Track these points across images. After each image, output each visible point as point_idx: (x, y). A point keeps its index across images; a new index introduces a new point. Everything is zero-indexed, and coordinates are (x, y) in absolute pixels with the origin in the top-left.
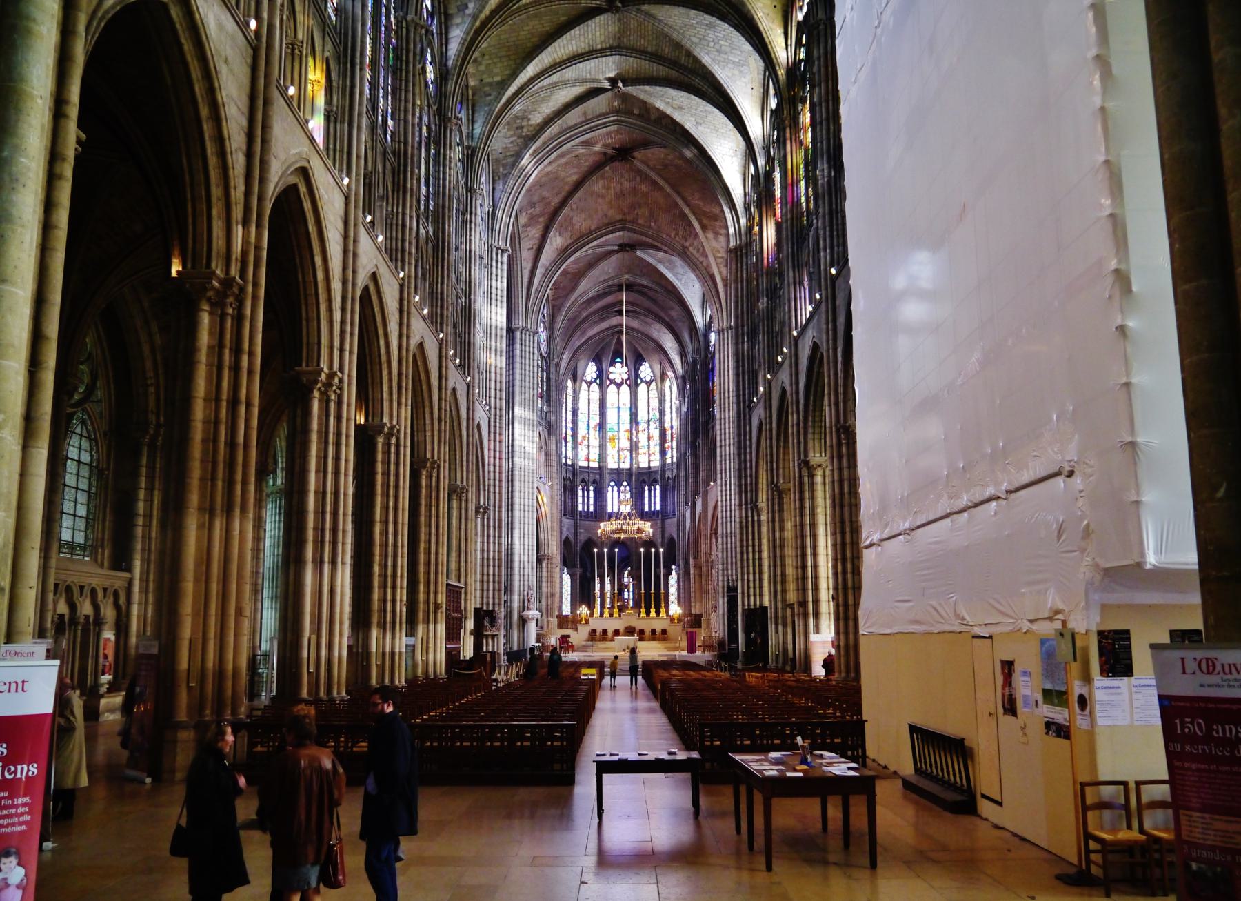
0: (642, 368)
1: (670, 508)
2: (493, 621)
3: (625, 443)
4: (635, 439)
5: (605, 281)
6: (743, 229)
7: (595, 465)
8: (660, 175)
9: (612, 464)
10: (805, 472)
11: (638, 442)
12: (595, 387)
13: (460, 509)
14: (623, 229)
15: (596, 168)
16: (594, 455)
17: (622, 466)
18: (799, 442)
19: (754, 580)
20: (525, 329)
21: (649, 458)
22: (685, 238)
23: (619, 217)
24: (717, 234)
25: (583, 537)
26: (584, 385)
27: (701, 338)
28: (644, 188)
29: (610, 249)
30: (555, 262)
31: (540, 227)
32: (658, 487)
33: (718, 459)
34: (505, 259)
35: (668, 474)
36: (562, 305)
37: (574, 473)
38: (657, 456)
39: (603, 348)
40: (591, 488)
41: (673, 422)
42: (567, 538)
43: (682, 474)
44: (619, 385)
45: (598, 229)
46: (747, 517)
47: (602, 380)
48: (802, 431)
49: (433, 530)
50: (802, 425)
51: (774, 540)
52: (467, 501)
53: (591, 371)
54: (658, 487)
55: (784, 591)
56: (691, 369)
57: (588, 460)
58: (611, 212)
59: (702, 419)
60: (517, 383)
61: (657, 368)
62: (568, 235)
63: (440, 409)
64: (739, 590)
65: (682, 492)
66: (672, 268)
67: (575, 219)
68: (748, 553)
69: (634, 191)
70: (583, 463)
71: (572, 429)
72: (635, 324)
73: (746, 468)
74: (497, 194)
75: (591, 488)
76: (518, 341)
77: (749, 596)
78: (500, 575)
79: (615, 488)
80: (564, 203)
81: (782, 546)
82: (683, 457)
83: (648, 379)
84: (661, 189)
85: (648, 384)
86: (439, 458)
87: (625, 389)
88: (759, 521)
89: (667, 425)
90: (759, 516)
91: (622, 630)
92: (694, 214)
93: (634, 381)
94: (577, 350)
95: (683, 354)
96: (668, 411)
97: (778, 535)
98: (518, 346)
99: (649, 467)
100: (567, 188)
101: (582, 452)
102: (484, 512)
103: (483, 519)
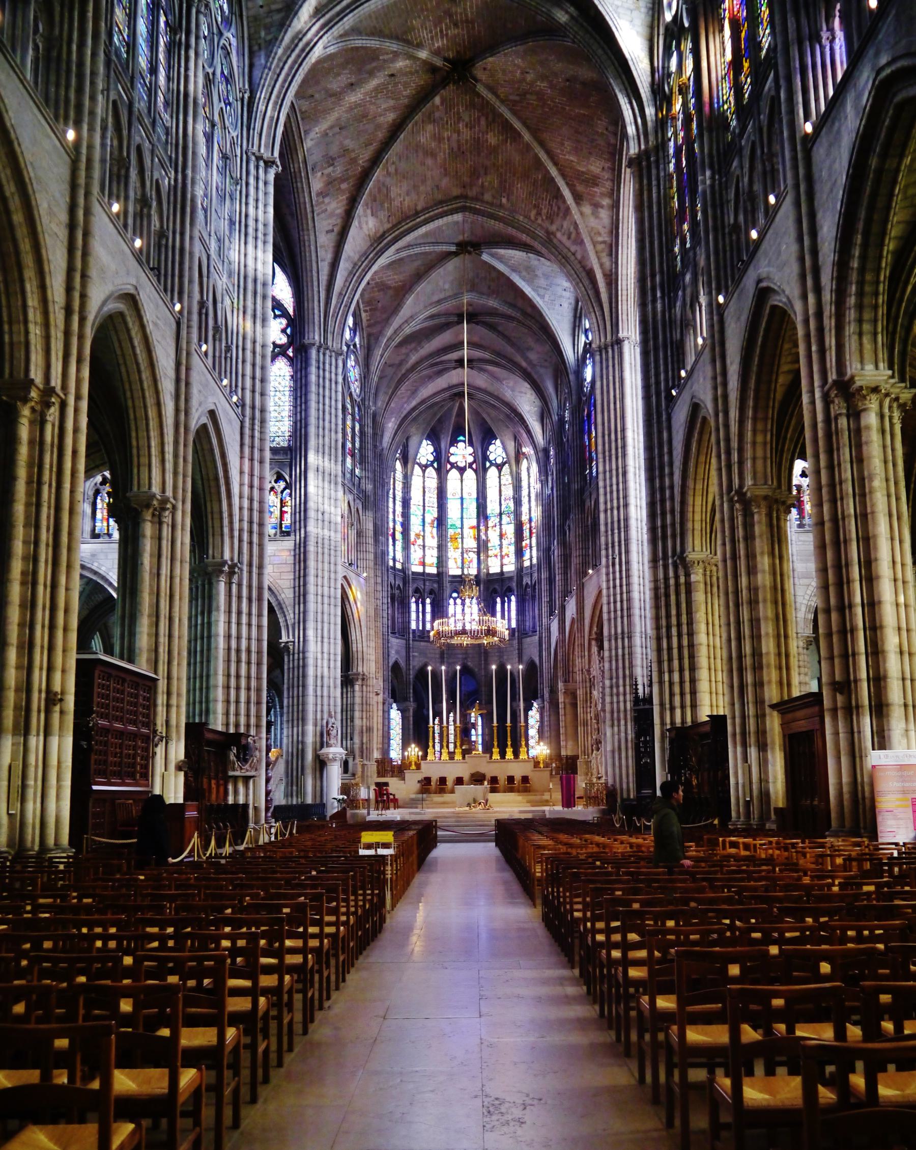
0: (492, 448)
1: (529, 624)
2: (245, 752)
3: (471, 543)
4: (483, 537)
5: (439, 302)
6: (650, 124)
7: (433, 570)
8: (515, 113)
10: (839, 406)
11: (488, 541)
12: (431, 472)
13: (160, 539)
14: (463, 209)
15: (421, 98)
16: (432, 557)
18: (822, 351)
19: (682, 682)
20: (323, 347)
21: (502, 561)
22: (551, 218)
23: (456, 192)
24: (596, 206)
25: (416, 663)
26: (417, 470)
27: (572, 377)
28: (492, 139)
29: (445, 248)
30: (365, 255)
31: (344, 198)
32: (513, 598)
33: (602, 528)
34: (271, 177)
35: (526, 580)
36: (381, 333)
37: (405, 580)
38: (512, 558)
39: (440, 421)
40: (428, 601)
41: (532, 512)
42: (396, 664)
43: (544, 575)
44: (462, 470)
45: (426, 210)
46: (666, 578)
47: (441, 463)
48: (829, 323)
49: (45, 536)
50: (829, 309)
51: (737, 592)
52: (174, 527)
53: (426, 452)
54: (513, 598)
55: (759, 685)
56: (557, 434)
57: (423, 564)
58: (445, 182)
59: (575, 486)
60: (312, 420)
61: (511, 446)
62: (383, 215)
63: (69, 289)
64: (656, 700)
65: (545, 599)
66: (531, 279)
68: (669, 637)
69: (478, 145)
71: (403, 525)
72: (481, 381)
73: (663, 501)
74: (257, 73)
75: (428, 601)
76: (314, 362)
77: (672, 709)
78: (259, 678)
79: (459, 601)
80: (375, 161)
81: (753, 603)
82: (546, 552)
83: (499, 461)
84: (516, 136)
85: (499, 467)
86: (64, 387)
87: (470, 474)
88: (688, 584)
89: (525, 518)
90: (688, 575)
91: (466, 778)
92: (564, 176)
93: (481, 465)
94: (406, 417)
95: (544, 415)
96: (525, 500)
97: (744, 581)
98: (313, 369)
99: (502, 573)
100: (380, 135)
101: (416, 554)
102: (231, 573)
103: (229, 584)
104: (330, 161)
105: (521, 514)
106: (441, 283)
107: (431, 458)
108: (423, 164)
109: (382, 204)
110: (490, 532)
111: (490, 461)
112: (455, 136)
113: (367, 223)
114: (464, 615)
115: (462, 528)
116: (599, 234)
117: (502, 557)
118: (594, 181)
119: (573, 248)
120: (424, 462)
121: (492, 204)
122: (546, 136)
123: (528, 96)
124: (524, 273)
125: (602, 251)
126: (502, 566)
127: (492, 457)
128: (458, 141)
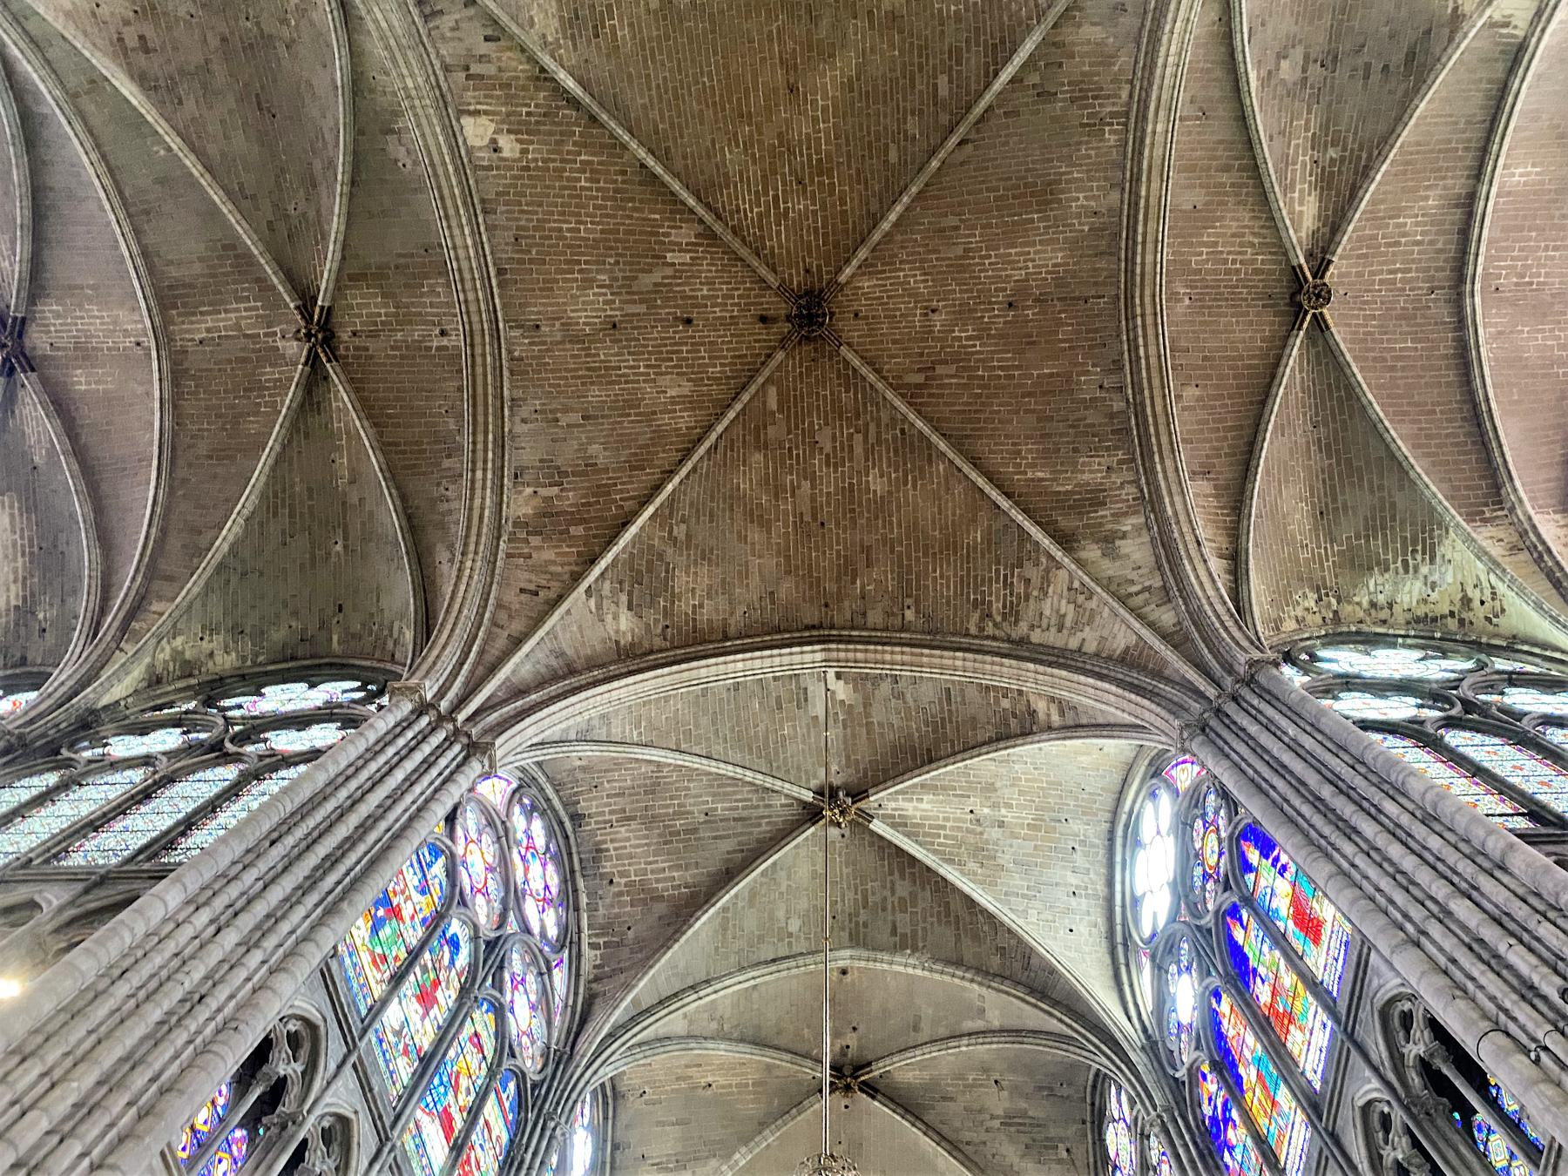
22: (1012, 613)
23: (811, 615)
67: (681, 581)
104: (556, 475)
106: (781, 914)
108: (743, 538)
109: (653, 597)
112: (806, 485)
113: (616, 617)
116: (1132, 582)
118: (1095, 498)
119: (1073, 643)
121: (886, 629)
122: (981, 447)
123: (940, 370)
124: (972, 865)
125: (1147, 603)
128: (813, 499)
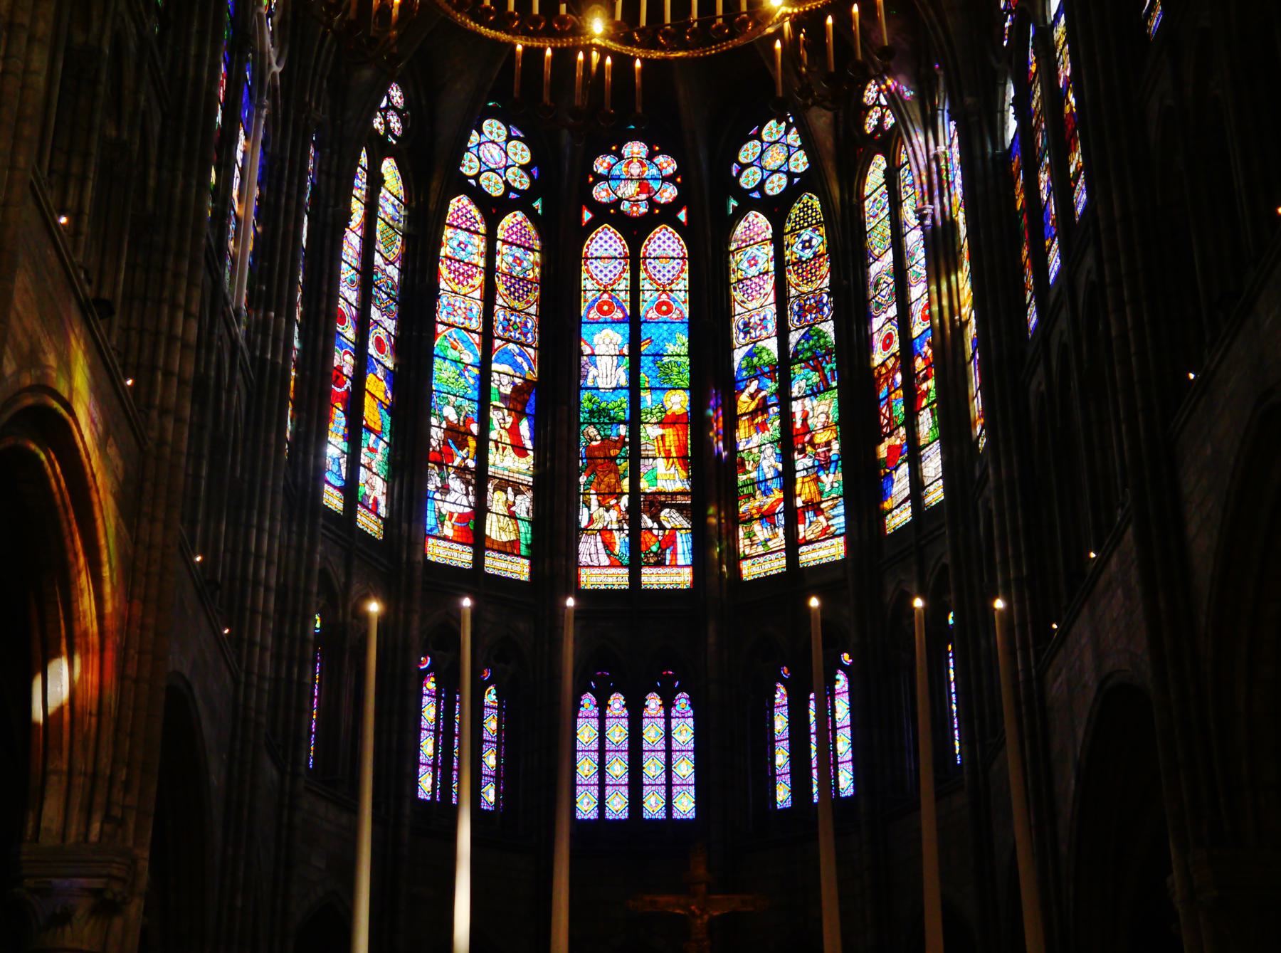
0: (748, 152)
3: (665, 476)
7: (520, 569)
9: (599, 570)
11: (735, 463)
17: (652, 578)
21: (795, 534)
32: (842, 682)
41: (921, 301)
44: (636, 232)
54: (842, 682)
70: (446, 551)
71: (393, 379)
79: (617, 703)
83: (776, 185)
85: (777, 209)
87: (665, 245)
101: (449, 501)
105: (868, 347)
107: (523, 183)
110: (741, 433)
111: (742, 195)
114: (636, 761)
115: (635, 422)
117: (793, 517)
120: (494, 186)
126: (793, 545)
127: (749, 180)
